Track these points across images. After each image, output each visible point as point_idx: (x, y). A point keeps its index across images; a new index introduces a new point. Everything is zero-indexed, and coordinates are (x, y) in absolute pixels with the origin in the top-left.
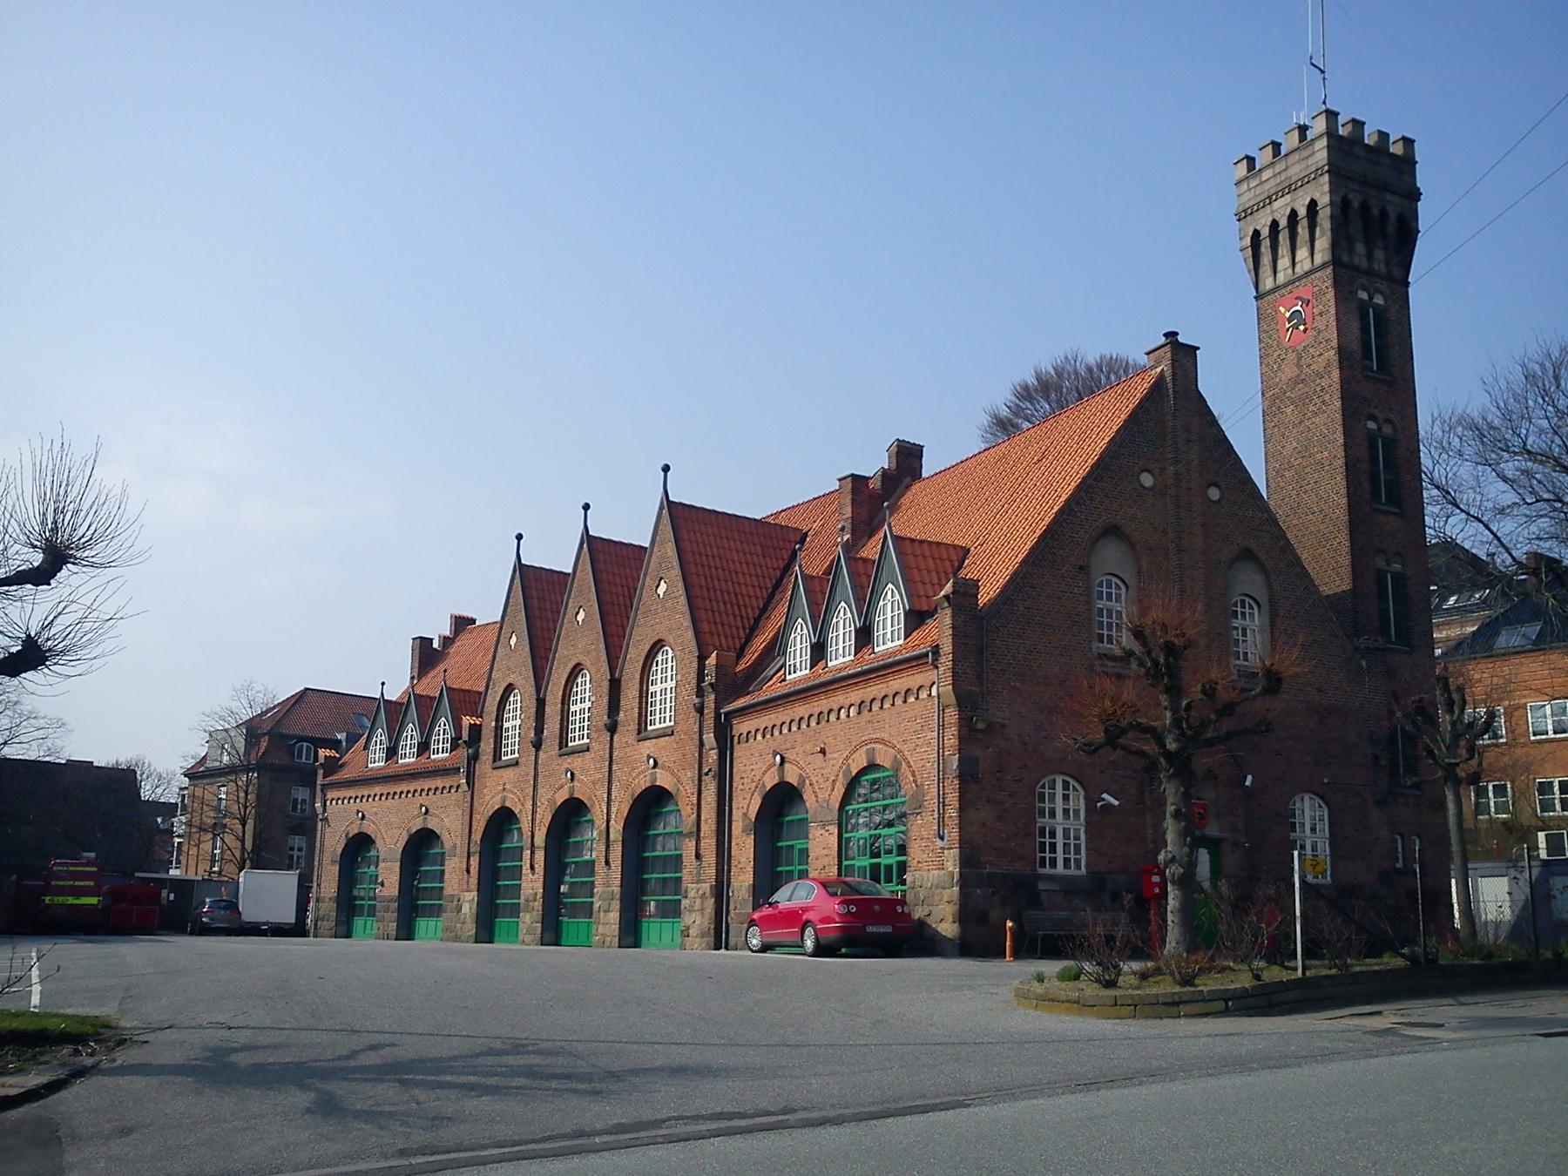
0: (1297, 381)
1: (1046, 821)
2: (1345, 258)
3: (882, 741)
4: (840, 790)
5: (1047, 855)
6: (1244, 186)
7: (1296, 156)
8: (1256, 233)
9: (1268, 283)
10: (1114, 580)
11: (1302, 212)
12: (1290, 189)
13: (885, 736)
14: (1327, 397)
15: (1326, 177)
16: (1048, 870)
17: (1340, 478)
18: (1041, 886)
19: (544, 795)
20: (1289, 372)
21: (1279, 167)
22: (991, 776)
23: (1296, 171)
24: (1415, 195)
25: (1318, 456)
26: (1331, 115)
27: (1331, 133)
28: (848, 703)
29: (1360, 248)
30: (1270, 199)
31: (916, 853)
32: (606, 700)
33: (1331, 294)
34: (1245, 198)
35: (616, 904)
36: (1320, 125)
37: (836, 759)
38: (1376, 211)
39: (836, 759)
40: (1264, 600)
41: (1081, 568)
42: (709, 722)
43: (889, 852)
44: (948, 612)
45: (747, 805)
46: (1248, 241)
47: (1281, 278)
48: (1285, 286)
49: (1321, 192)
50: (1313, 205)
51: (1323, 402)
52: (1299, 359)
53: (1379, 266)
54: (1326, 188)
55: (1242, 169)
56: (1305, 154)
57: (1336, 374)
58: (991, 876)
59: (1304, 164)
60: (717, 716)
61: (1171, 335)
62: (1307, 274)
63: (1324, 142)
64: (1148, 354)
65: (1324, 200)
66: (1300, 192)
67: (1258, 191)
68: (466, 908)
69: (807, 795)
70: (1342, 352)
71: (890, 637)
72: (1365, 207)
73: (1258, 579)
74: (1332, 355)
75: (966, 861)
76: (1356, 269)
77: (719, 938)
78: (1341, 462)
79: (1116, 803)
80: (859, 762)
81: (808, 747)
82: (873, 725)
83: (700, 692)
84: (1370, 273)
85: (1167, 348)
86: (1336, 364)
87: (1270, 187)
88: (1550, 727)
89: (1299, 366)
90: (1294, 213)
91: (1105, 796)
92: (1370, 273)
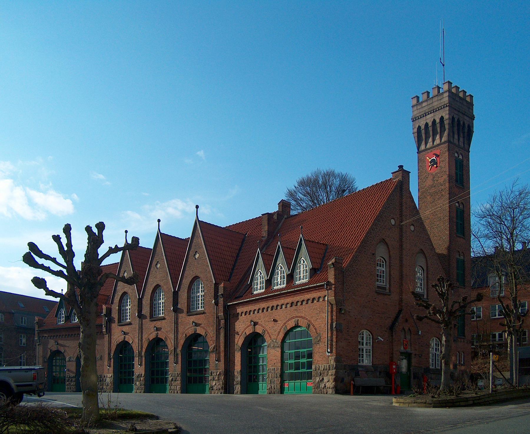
0: (432, 186)
1: (360, 347)
2: (452, 141)
3: (301, 317)
4: (281, 335)
5: (361, 358)
6: (415, 108)
7: (436, 99)
8: (419, 127)
9: (423, 147)
10: (382, 259)
11: (438, 121)
12: (434, 111)
13: (303, 315)
14: (443, 193)
15: (448, 108)
16: (361, 364)
17: (447, 224)
18: (360, 369)
19: (145, 336)
20: (429, 182)
21: (429, 102)
22: (343, 331)
23: (436, 104)
24: (473, 118)
25: (439, 215)
26: (450, 83)
27: (449, 91)
28: (286, 302)
29: (456, 136)
30: (426, 115)
31: (316, 357)
32: (172, 299)
33: (447, 154)
34: (415, 113)
35: (179, 378)
36: (446, 87)
37: (280, 323)
38: (462, 123)
39: (280, 323)
40: (425, 269)
41: (373, 254)
42: (221, 308)
43: (303, 357)
44: (333, 269)
45: (239, 341)
46: (416, 130)
47: (428, 146)
48: (429, 149)
49: (445, 114)
50: (442, 118)
51: (442, 195)
52: (434, 178)
53: (461, 144)
54: (447, 112)
55: (415, 101)
56: (439, 98)
57: (447, 185)
58: (345, 365)
59: (439, 102)
60: (224, 307)
61: (401, 167)
62: (438, 145)
63: (447, 94)
64: (392, 173)
65: (446, 117)
66: (437, 113)
67: (421, 110)
68: (108, 380)
69: (266, 337)
70: (449, 176)
71: (303, 277)
72: (459, 121)
73: (424, 260)
74: (446, 177)
75: (337, 360)
76: (455, 144)
77: (228, 388)
78: (447, 218)
79: (382, 340)
80: (291, 324)
81: (267, 319)
82: (293, 310)
83: (216, 297)
84: (459, 146)
85: (400, 172)
86: (447, 181)
87: (426, 109)
88: (497, 314)
89: (433, 181)
90: (434, 121)
91: (379, 337)
92: (459, 146)
